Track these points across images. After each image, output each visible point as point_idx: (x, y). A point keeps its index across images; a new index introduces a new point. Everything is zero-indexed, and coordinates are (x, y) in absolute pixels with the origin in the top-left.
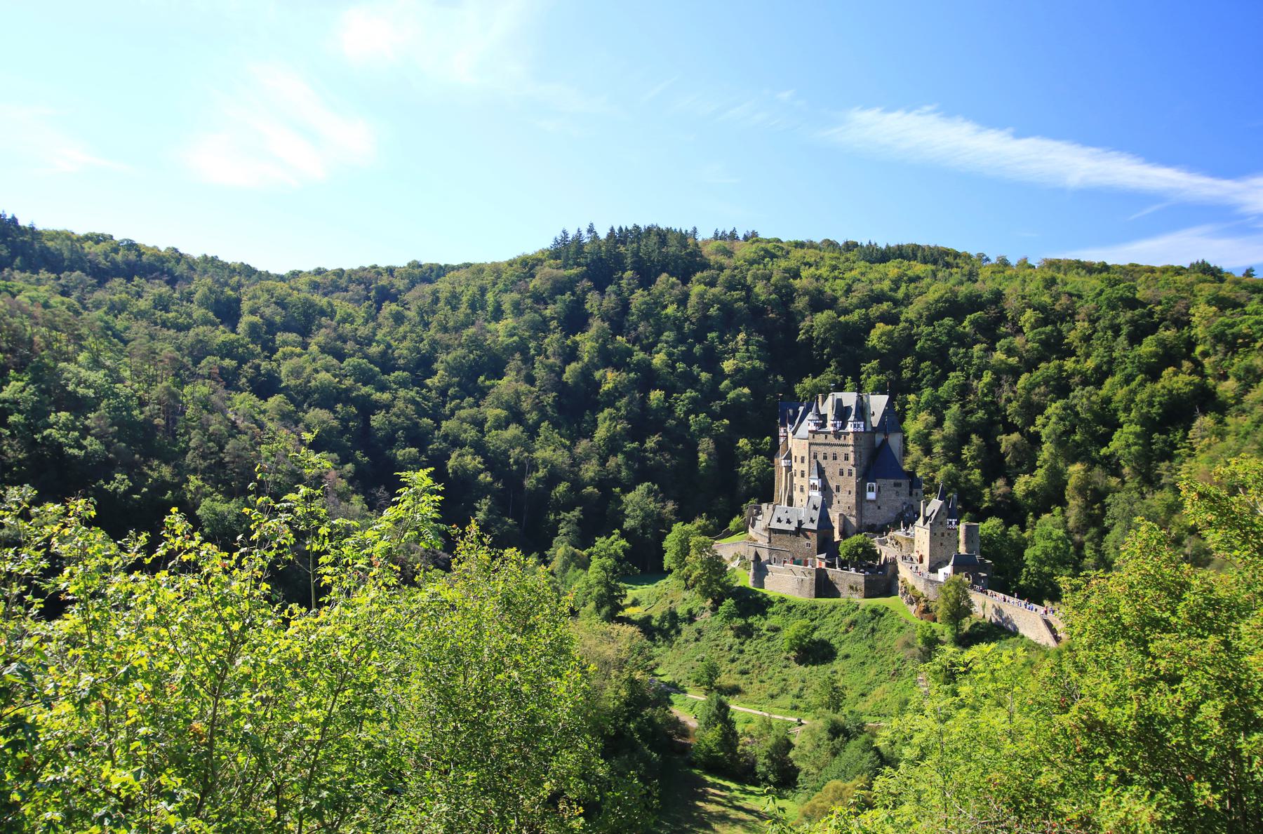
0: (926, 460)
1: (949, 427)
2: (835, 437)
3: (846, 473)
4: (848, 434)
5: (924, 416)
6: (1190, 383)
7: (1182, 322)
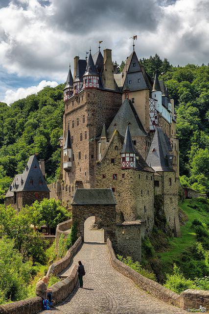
3: (84, 136)
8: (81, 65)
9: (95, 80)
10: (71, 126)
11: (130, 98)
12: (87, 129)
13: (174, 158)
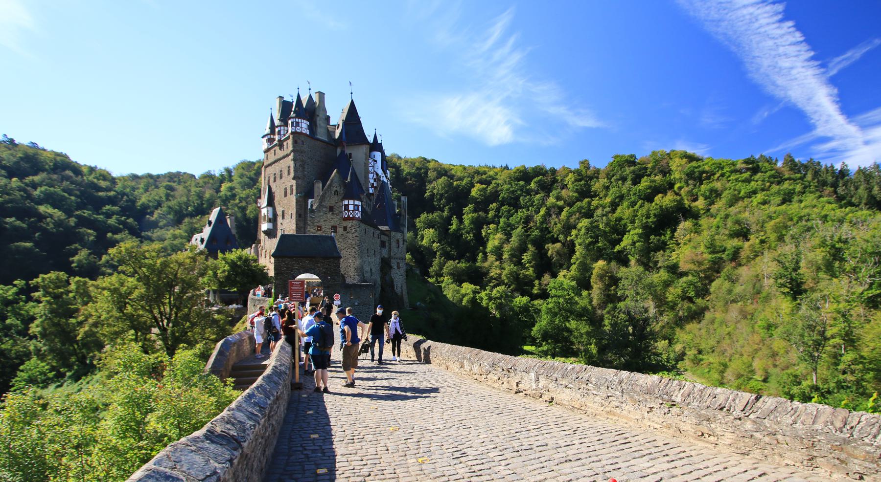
0: (497, 263)
1: (515, 240)
3: (289, 192)
5: (499, 235)
6: (674, 201)
7: (666, 172)
11: (348, 151)
12: (294, 182)
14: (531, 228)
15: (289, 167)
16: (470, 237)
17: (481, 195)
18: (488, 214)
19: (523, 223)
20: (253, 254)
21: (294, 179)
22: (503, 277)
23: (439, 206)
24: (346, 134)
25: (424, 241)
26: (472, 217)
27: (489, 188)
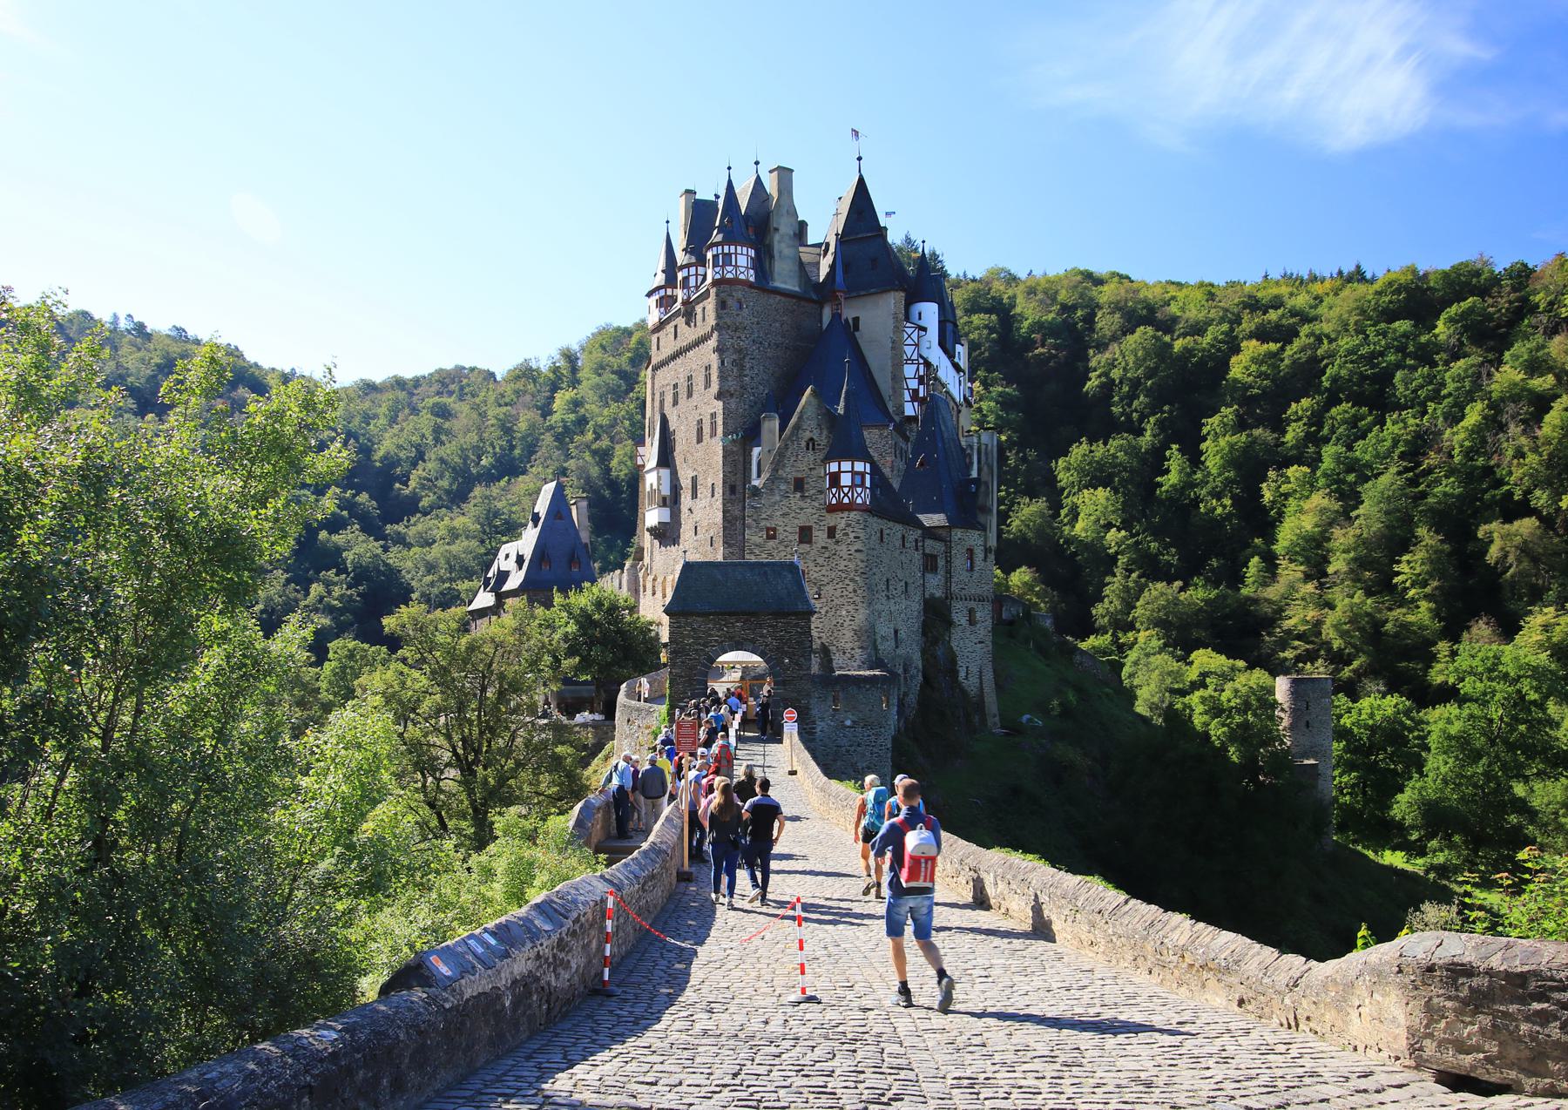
0: (1310, 587)
1: (1370, 513)
2: (688, 324)
3: (707, 430)
4: (706, 295)
5: (1318, 500)
8: (700, 213)
9: (743, 258)
10: (669, 399)
11: (848, 313)
12: (720, 404)
13: (983, 488)
14: (1430, 471)
15: (708, 368)
16: (1223, 507)
17: (1260, 375)
18: (1284, 432)
19: (1402, 456)
20: (625, 593)
21: (719, 396)
22: (1328, 632)
23: (1129, 416)
24: (847, 267)
25: (1079, 526)
26: (1232, 446)
27: (1289, 351)
